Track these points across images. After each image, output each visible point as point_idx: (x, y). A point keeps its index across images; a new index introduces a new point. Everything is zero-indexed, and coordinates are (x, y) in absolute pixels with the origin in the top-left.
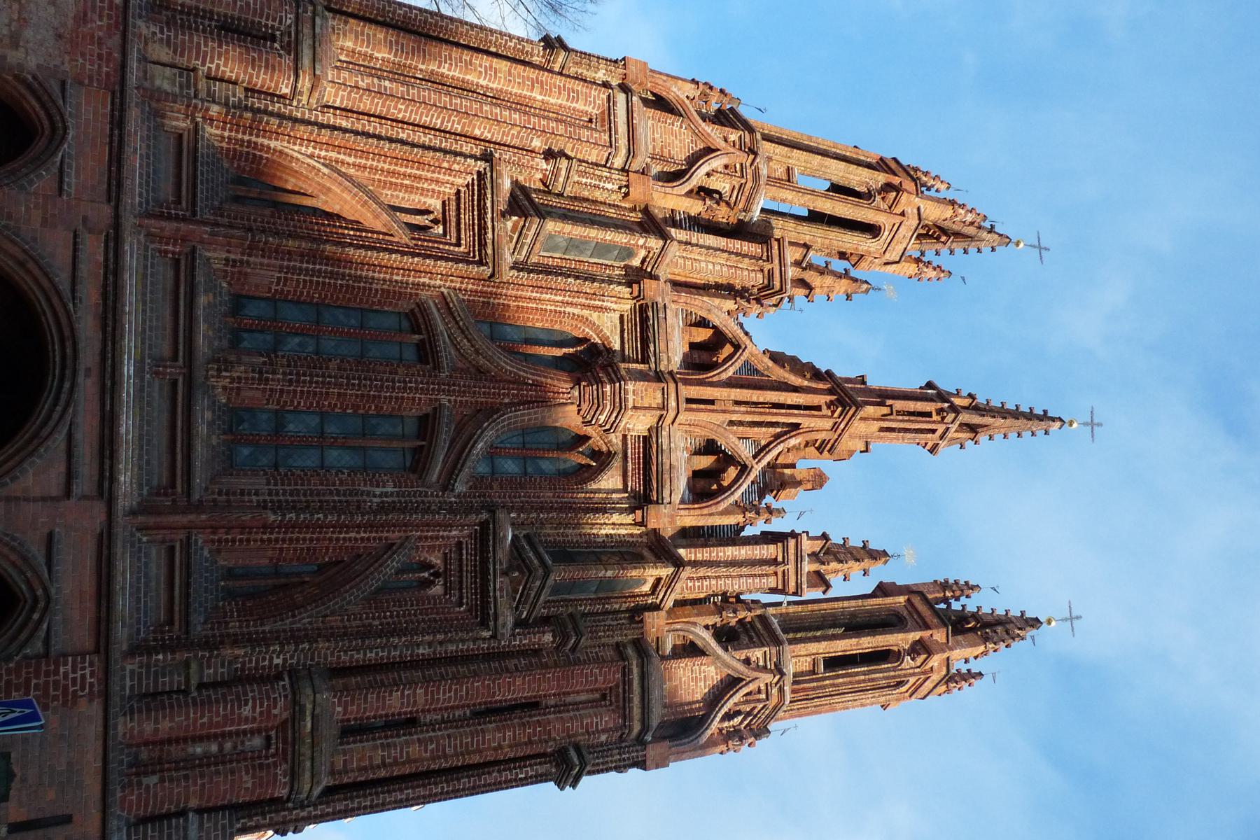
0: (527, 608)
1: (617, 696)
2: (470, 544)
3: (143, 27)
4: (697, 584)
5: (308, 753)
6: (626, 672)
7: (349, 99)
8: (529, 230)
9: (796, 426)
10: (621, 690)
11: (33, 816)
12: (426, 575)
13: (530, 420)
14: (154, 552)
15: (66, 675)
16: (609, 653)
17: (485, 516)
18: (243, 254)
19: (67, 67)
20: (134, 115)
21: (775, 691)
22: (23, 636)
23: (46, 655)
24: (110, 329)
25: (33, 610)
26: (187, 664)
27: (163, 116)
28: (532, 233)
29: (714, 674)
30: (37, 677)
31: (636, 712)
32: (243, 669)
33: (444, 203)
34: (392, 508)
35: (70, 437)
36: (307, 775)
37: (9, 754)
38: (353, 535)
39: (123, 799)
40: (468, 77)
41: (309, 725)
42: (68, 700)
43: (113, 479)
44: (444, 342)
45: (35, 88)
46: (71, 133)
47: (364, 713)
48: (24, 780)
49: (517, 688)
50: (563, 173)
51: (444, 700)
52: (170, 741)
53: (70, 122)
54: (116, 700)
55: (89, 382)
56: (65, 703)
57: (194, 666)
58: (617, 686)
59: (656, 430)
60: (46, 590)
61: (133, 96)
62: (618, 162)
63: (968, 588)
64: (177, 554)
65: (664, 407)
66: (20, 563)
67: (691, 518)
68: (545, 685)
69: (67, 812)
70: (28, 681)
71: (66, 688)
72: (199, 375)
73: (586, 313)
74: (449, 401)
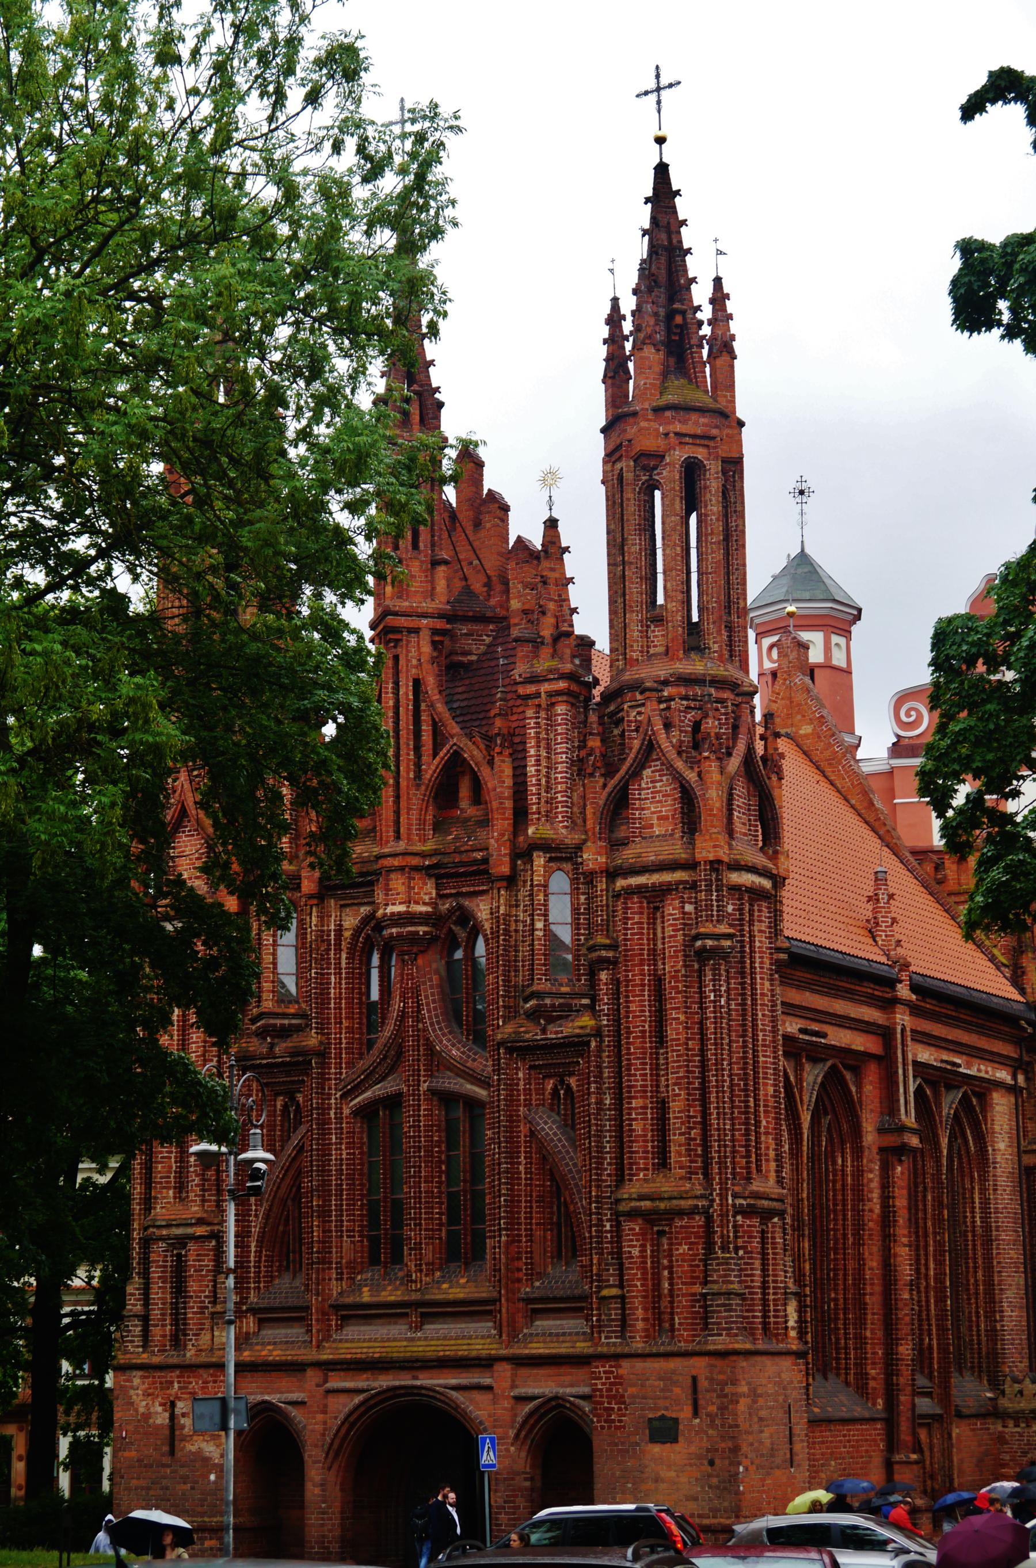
0: (576, 1001)
1: (654, 897)
3: (190, 1354)
9: (417, 683)
11: (690, 1402)
13: (434, 1001)
14: (538, 1323)
15: (603, 1384)
18: (330, 1269)
26: (604, 1298)
27: (248, 1333)
28: (278, 1022)
30: (602, 1403)
31: (667, 877)
32: (612, 1253)
36: (682, 1203)
37: (650, 1419)
38: (522, 1168)
39: (686, 1341)
42: (619, 1381)
43: (478, 1358)
44: (380, 1089)
46: (267, 1398)
47: (647, 1152)
52: (654, 1308)
53: (259, 1398)
54: (619, 1350)
55: (421, 1376)
56: (621, 1384)
57: (605, 1292)
59: (427, 871)
63: (614, 319)
65: (401, 869)
66: (535, 1417)
68: (638, 975)
69: (690, 1380)
70: (606, 1409)
71: (611, 1384)
72: (415, 1297)
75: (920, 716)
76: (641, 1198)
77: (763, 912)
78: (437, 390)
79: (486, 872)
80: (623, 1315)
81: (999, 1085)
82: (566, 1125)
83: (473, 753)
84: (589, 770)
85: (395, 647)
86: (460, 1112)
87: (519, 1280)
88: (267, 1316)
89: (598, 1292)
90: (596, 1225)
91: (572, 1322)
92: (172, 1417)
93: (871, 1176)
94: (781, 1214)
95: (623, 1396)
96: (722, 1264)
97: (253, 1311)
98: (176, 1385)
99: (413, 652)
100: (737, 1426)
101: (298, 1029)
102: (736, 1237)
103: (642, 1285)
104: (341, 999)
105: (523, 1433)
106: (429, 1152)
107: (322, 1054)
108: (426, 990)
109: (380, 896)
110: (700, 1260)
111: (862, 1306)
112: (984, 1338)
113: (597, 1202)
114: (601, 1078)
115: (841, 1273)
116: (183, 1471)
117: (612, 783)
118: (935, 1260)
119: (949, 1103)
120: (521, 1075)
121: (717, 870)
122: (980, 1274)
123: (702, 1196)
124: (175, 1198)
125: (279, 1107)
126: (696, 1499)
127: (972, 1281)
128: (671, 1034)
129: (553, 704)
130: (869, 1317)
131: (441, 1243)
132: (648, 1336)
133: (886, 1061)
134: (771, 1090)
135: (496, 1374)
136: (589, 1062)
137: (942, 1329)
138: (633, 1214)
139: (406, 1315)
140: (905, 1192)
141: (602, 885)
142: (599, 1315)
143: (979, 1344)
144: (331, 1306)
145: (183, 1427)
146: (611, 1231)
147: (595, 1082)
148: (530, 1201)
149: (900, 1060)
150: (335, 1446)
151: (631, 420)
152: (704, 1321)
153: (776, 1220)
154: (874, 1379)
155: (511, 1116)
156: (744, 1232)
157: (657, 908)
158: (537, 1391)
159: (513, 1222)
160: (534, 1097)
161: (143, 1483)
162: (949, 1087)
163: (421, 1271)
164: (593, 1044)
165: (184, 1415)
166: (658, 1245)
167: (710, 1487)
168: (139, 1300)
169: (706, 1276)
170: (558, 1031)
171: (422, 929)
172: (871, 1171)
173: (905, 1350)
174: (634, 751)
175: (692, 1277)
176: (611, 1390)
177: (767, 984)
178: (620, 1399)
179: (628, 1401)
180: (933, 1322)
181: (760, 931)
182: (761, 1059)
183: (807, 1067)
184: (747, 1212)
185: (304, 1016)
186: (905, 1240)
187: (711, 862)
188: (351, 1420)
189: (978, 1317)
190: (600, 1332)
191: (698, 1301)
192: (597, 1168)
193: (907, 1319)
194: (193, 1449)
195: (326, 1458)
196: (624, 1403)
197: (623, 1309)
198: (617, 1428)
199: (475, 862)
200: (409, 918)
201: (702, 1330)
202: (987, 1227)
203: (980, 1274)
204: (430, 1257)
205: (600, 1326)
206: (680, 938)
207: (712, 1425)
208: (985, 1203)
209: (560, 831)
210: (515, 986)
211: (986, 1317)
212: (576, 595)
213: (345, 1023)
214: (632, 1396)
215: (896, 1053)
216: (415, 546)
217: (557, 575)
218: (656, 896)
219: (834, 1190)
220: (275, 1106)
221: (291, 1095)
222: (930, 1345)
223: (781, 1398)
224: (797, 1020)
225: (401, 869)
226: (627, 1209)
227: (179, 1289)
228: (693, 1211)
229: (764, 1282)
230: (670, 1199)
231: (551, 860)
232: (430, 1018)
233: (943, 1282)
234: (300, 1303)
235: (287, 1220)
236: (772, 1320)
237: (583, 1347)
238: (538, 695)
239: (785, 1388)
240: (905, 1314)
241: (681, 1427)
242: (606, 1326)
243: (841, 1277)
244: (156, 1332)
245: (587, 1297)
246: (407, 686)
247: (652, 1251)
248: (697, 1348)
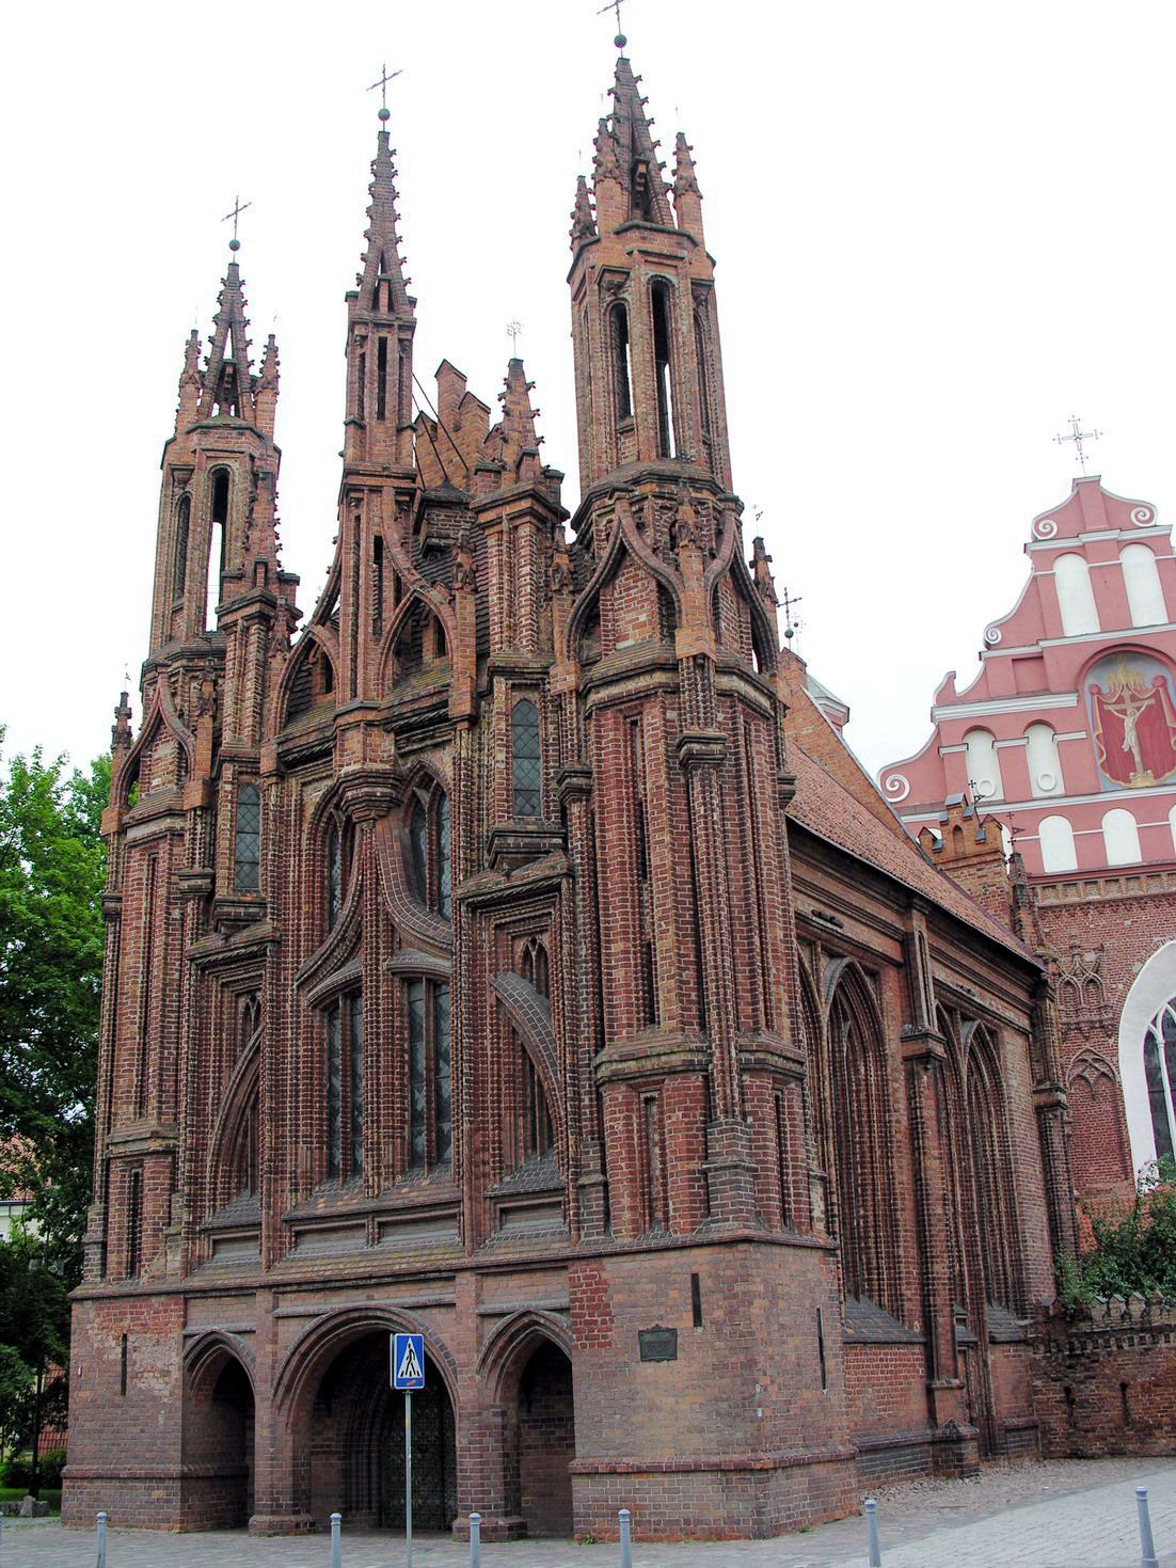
0: (546, 841)
3: (145, 1278)
4: (524, 634)
5: (654, 1060)
6: (603, 707)
7: (169, 1102)
8: (229, 914)
9: (379, 542)
10: (622, 707)
11: (690, 1307)
12: (534, 954)
13: (394, 870)
15: (584, 1292)
19: (175, 1335)
20: (196, 1282)
22: (557, 1330)
23: (568, 1309)
24: (338, 1284)
25: (538, 1323)
26: (583, 1187)
29: (623, 578)
30: (584, 1315)
31: (643, 682)
33: (238, 996)
37: (641, 1333)
38: (487, 1043)
39: (683, 1231)
40: (139, 994)
41: (632, 1064)
42: (602, 1287)
46: (216, 1328)
47: (631, 1005)
48: (661, 1318)
50: (192, 882)
51: (622, 920)
52: (643, 1194)
53: (209, 1328)
54: (602, 1249)
56: (605, 1291)
57: (584, 1180)
58: (621, 711)
59: (385, 725)
60: (523, 1315)
62: (178, 823)
64: (506, 1205)
65: (357, 725)
68: (612, 798)
69: (689, 1278)
70: (587, 1322)
72: (372, 1204)
73: (306, 826)
74: (384, 960)
75: (902, 786)
77: (761, 732)
78: (408, 281)
80: (607, 1207)
81: (1009, 1023)
82: (540, 993)
83: (435, 596)
84: (556, 587)
85: (357, 507)
86: (421, 991)
87: (485, 1175)
88: (222, 1237)
89: (577, 1180)
90: (573, 1099)
93: (896, 1085)
94: (800, 1078)
95: (608, 1305)
96: (726, 1131)
99: (376, 510)
100: (751, 1333)
101: (254, 920)
102: (743, 1101)
103: (628, 1166)
104: (300, 883)
105: (491, 1358)
106: (390, 1040)
107: (277, 942)
108: (385, 859)
110: (698, 1129)
111: (893, 1224)
112: (1009, 1269)
113: (573, 1072)
114: (575, 926)
115: (870, 1188)
116: (134, 1412)
117: (579, 598)
118: (961, 1186)
119: (966, 1032)
120: (485, 936)
121: (702, 666)
122: (1002, 1204)
123: (699, 1050)
124: (135, 1113)
125: (241, 1009)
126: (701, 1431)
127: (995, 1212)
128: (654, 860)
129: (516, 528)
130: (902, 1234)
131: (403, 1144)
132: (637, 1230)
133: (905, 966)
134: (780, 934)
135: (458, 1288)
136: (560, 910)
137: (972, 1255)
139: (363, 1226)
140: (932, 1102)
141: (571, 706)
142: (578, 1208)
143: (1005, 1274)
144: (286, 1221)
146: (591, 1106)
147: (569, 930)
148: (498, 1082)
149: (920, 965)
150: (285, 1381)
151: (594, 247)
152: (705, 1205)
153: (793, 1085)
154: (909, 1300)
155: (474, 984)
156: (756, 1094)
157: (634, 723)
159: (477, 1108)
160: (501, 962)
162: (965, 1018)
163: (379, 1174)
166: (646, 1116)
167: (718, 1414)
168: (99, 1225)
169: (706, 1150)
171: (379, 791)
172: (896, 1081)
173: (940, 1269)
174: (604, 560)
175: (689, 1151)
176: (592, 1299)
177: (770, 814)
178: (604, 1309)
179: (613, 1312)
180: (963, 1248)
181: (759, 753)
182: (767, 896)
183: (824, 961)
184: (757, 1069)
185: (262, 905)
186: (936, 1153)
187: (695, 657)
188: (301, 1352)
189: (1002, 1248)
190: (579, 1229)
191: (698, 1180)
192: (572, 1031)
193: (943, 1234)
195: (275, 1395)
196: (609, 1314)
197: (606, 1198)
198: (600, 1345)
200: (365, 778)
201: (703, 1216)
202: (1006, 1161)
203: (1002, 1204)
205: (579, 1222)
206: (662, 749)
208: (1003, 1137)
209: (525, 656)
210: (478, 837)
211: (1010, 1247)
212: (540, 427)
213: (305, 908)
214: (620, 1305)
215: (915, 958)
216: (381, 415)
217: (521, 408)
219: (858, 1101)
220: (236, 1008)
221: (251, 993)
222: (961, 1274)
223: (807, 1303)
224: (809, 900)
225: (357, 725)
226: (608, 1073)
227: (135, 1213)
228: (688, 1069)
229: (781, 1159)
230: (659, 1055)
232: (389, 888)
233: (970, 1208)
234: (252, 1219)
235: (246, 1132)
236: (793, 1206)
237: (558, 1249)
239: (812, 1291)
240: (938, 1231)
241: (679, 1340)
242: (585, 1221)
243: (869, 1192)
244: (112, 1258)
245: (563, 1189)
246: (367, 543)
247: (639, 1124)
248: (700, 1238)
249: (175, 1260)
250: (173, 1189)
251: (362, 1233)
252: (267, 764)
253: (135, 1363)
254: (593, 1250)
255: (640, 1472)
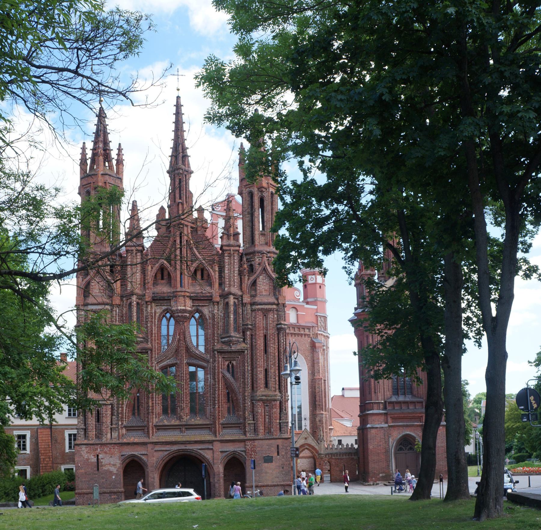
2: (223, 355)
6: (259, 310)
16: (254, 314)
17: (216, 352)
20: (125, 441)
21: (269, 255)
34: (214, 377)
35: (200, 449)
45: (124, 461)
49: (260, 342)
53: (130, 453)
54: (255, 438)
57: (249, 422)
59: (190, 297)
61: (121, 441)
65: (184, 296)
67: (217, 285)
72: (184, 423)
73: (157, 318)
76: (263, 396)
79: (211, 300)
88: (129, 429)
91: (236, 431)
92: (98, 459)
97: (125, 427)
98: (99, 450)
107: (151, 350)
109: (173, 303)
138: (259, 400)
144: (155, 426)
145: (102, 462)
158: (225, 450)
161: (87, 479)
164: (246, 352)
165: (102, 459)
170: (234, 348)
178: (255, 452)
194: (106, 469)
199: (207, 296)
200: (185, 311)
204: (187, 412)
207: (283, 458)
214: (259, 450)
218: (265, 312)
227: (98, 419)
231: (234, 298)
237: (242, 437)
238: (230, 250)
249: (115, 435)
250: (112, 414)
251: (179, 430)
252: (148, 298)
253: (102, 462)
254: (253, 438)
255: (264, 486)
